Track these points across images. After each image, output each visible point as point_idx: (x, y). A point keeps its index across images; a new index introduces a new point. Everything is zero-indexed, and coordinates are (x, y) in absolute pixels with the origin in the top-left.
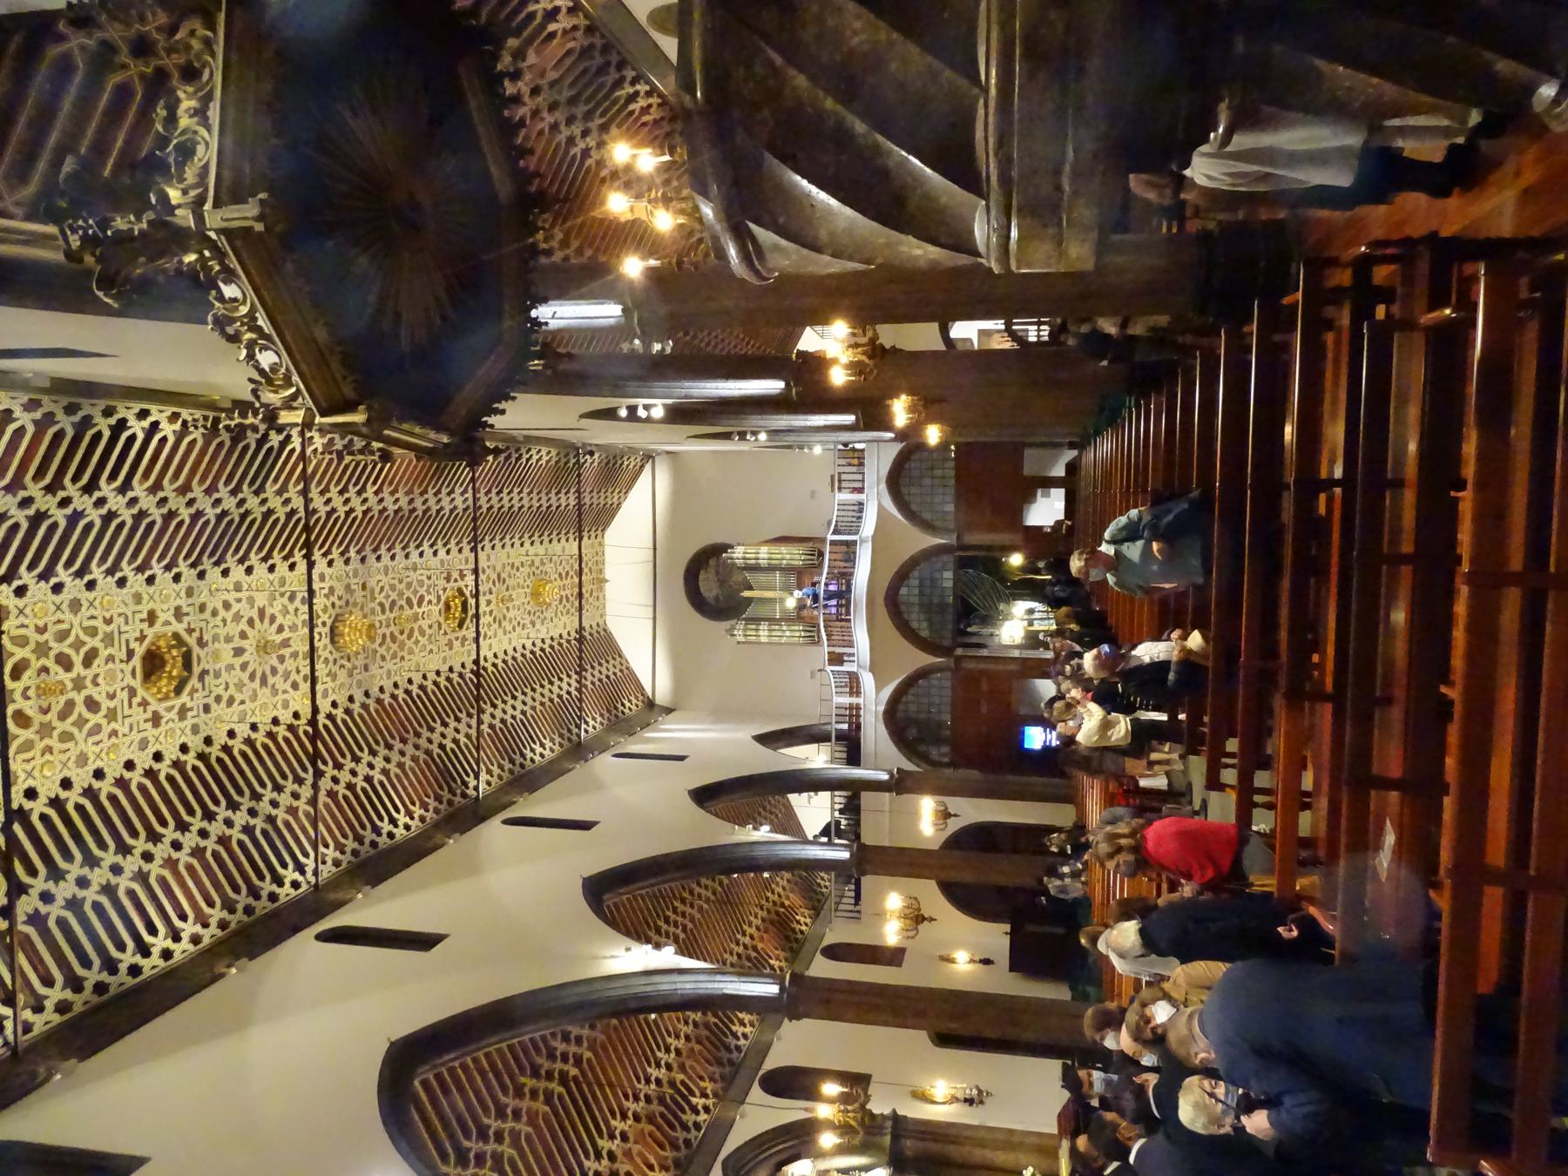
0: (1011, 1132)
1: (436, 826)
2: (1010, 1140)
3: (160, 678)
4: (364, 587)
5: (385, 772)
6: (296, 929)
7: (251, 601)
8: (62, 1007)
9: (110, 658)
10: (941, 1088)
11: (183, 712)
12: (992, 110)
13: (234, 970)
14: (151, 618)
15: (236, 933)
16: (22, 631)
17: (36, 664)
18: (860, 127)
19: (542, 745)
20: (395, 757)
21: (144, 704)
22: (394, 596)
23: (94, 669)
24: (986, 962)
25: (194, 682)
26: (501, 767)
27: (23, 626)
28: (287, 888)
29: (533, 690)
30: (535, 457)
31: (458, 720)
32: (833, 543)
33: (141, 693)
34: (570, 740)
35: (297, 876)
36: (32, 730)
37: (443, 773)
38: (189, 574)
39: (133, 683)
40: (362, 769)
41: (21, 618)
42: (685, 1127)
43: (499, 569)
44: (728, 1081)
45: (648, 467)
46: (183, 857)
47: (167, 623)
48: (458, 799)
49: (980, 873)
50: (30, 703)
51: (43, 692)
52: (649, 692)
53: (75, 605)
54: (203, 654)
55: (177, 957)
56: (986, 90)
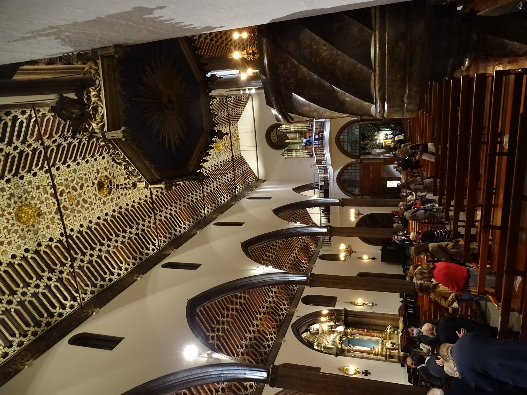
0: (383, 314)
2: (383, 317)
3: (103, 190)
5: (176, 211)
6: (156, 264)
8: (92, 293)
9: (88, 186)
10: (360, 301)
11: (112, 200)
12: (377, 78)
13: (139, 278)
14: (98, 172)
15: (138, 266)
16: (60, 181)
17: (66, 191)
18: (327, 84)
19: (224, 197)
20: (178, 206)
21: (100, 199)
23: (84, 190)
24: (374, 259)
26: (211, 206)
27: (60, 179)
28: (151, 251)
29: (219, 179)
31: (196, 192)
32: (316, 123)
34: (232, 194)
35: (153, 247)
36: (69, 211)
37: (193, 209)
39: (96, 193)
40: (169, 211)
41: (60, 177)
42: (279, 315)
44: (291, 300)
46: (119, 245)
47: (103, 173)
48: (199, 217)
49: (370, 229)
50: (67, 203)
51: (70, 199)
52: (257, 175)
55: (122, 275)
56: (375, 71)
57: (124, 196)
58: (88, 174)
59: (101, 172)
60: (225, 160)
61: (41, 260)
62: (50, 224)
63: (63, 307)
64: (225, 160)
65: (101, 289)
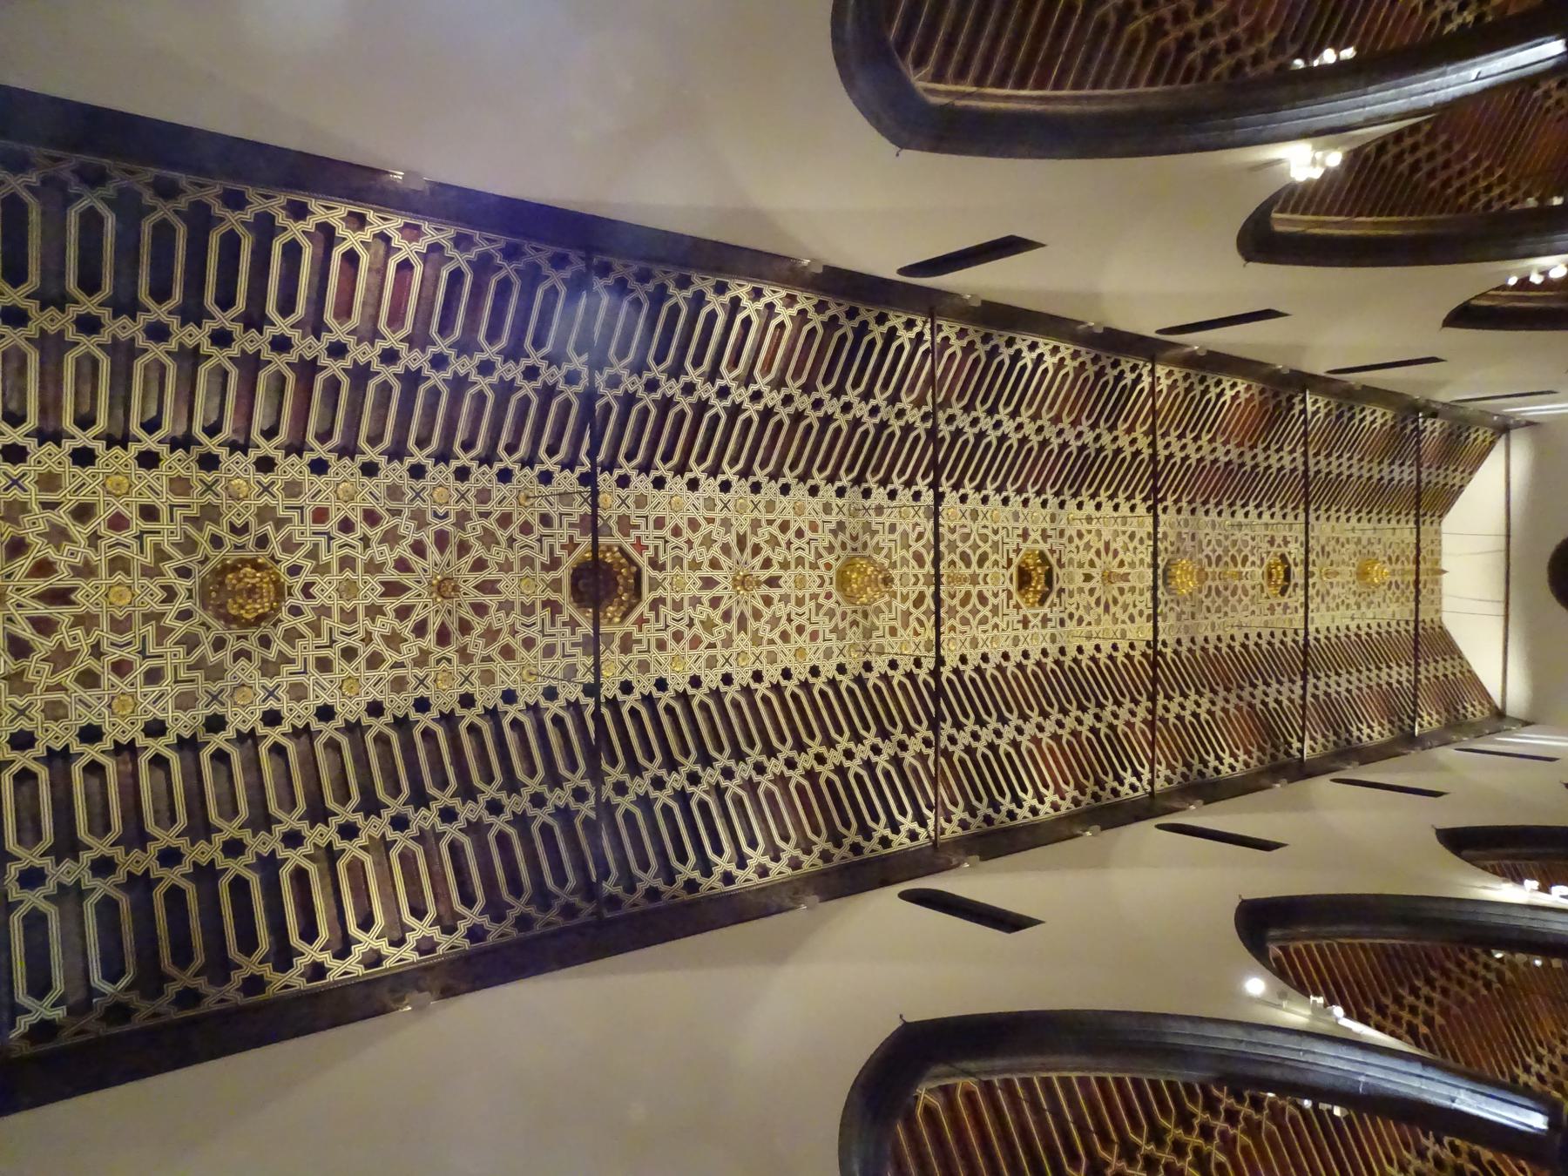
4: (1193, 537)
7: (1099, 533)
9: (996, 563)
19: (1370, 727)
21: (1017, 606)
22: (1220, 551)
25: (1053, 596)
26: (1324, 736)
30: (1369, 419)
37: (1265, 727)
38: (1053, 502)
43: (1323, 541)
45: (1500, 446)
47: (1036, 541)
48: (1281, 756)
52: (1497, 700)
53: (974, 515)
54: (1061, 573)
58: (1002, 533)
59: (1031, 539)
61: (865, 703)
62: (898, 624)
63: (895, 827)
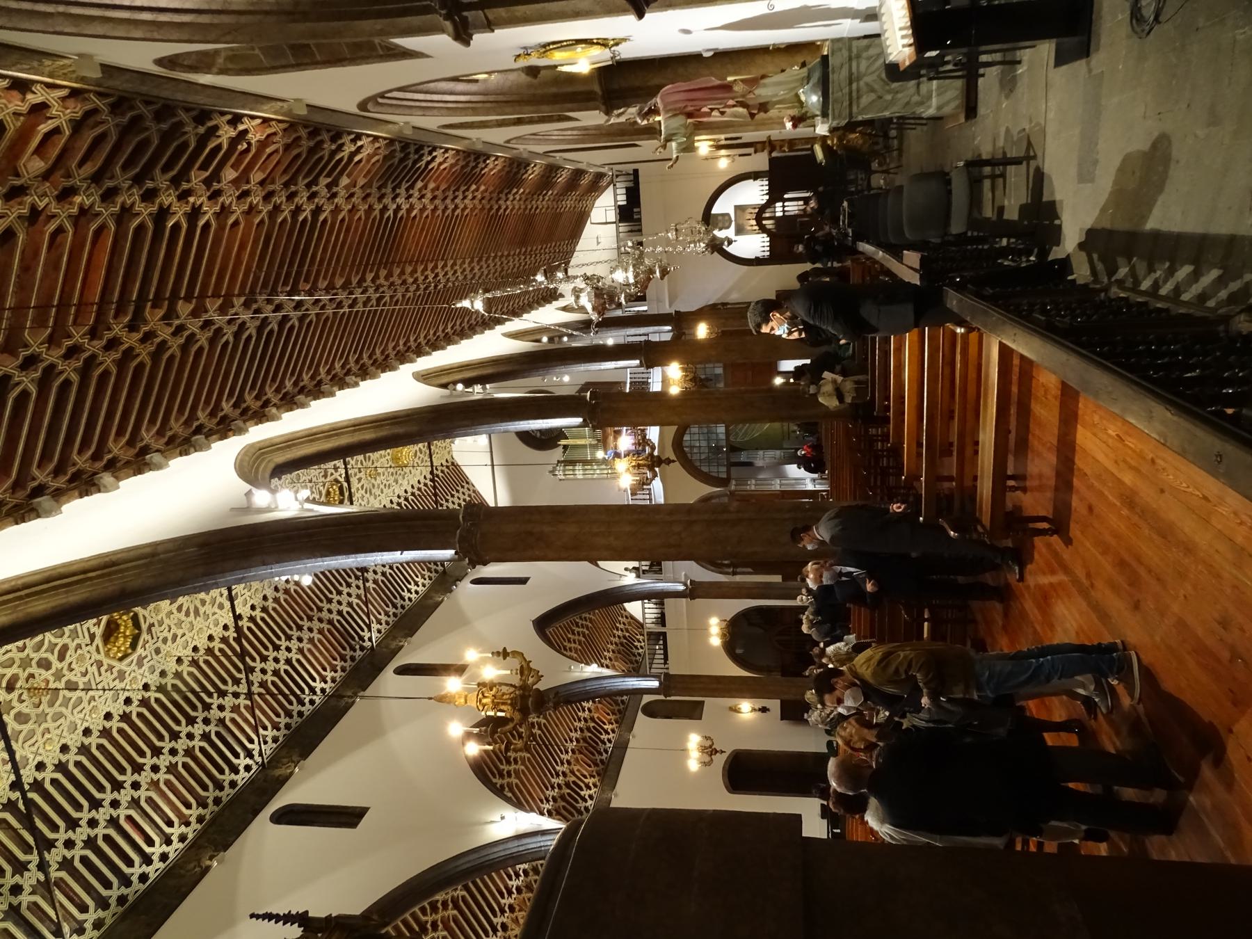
1: (345, 683)
3: (117, 638)
5: (301, 651)
6: (256, 813)
15: (213, 821)
23: (68, 659)
25: (145, 636)
26: (387, 614)
33: (106, 661)
34: (436, 571)
35: (248, 761)
36: (31, 722)
39: (99, 657)
48: (359, 653)
50: (25, 704)
57: (169, 642)
60: (416, 485)
64: (416, 485)
65: (120, 909)
